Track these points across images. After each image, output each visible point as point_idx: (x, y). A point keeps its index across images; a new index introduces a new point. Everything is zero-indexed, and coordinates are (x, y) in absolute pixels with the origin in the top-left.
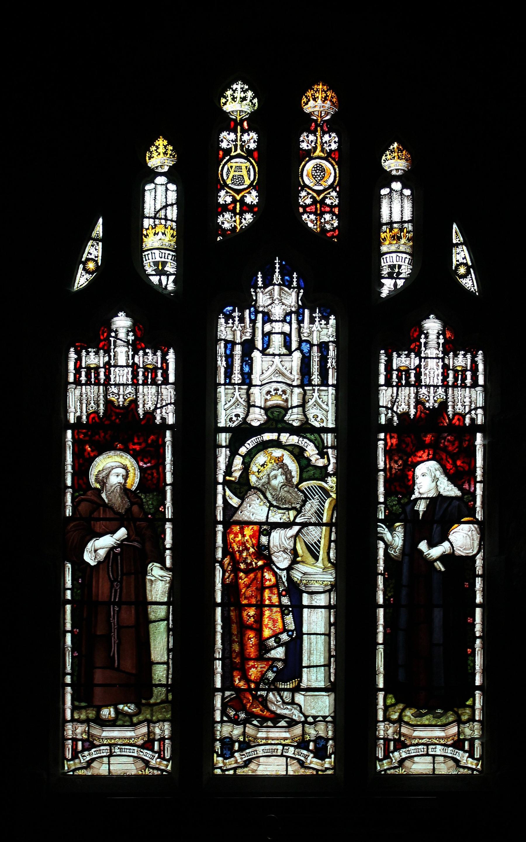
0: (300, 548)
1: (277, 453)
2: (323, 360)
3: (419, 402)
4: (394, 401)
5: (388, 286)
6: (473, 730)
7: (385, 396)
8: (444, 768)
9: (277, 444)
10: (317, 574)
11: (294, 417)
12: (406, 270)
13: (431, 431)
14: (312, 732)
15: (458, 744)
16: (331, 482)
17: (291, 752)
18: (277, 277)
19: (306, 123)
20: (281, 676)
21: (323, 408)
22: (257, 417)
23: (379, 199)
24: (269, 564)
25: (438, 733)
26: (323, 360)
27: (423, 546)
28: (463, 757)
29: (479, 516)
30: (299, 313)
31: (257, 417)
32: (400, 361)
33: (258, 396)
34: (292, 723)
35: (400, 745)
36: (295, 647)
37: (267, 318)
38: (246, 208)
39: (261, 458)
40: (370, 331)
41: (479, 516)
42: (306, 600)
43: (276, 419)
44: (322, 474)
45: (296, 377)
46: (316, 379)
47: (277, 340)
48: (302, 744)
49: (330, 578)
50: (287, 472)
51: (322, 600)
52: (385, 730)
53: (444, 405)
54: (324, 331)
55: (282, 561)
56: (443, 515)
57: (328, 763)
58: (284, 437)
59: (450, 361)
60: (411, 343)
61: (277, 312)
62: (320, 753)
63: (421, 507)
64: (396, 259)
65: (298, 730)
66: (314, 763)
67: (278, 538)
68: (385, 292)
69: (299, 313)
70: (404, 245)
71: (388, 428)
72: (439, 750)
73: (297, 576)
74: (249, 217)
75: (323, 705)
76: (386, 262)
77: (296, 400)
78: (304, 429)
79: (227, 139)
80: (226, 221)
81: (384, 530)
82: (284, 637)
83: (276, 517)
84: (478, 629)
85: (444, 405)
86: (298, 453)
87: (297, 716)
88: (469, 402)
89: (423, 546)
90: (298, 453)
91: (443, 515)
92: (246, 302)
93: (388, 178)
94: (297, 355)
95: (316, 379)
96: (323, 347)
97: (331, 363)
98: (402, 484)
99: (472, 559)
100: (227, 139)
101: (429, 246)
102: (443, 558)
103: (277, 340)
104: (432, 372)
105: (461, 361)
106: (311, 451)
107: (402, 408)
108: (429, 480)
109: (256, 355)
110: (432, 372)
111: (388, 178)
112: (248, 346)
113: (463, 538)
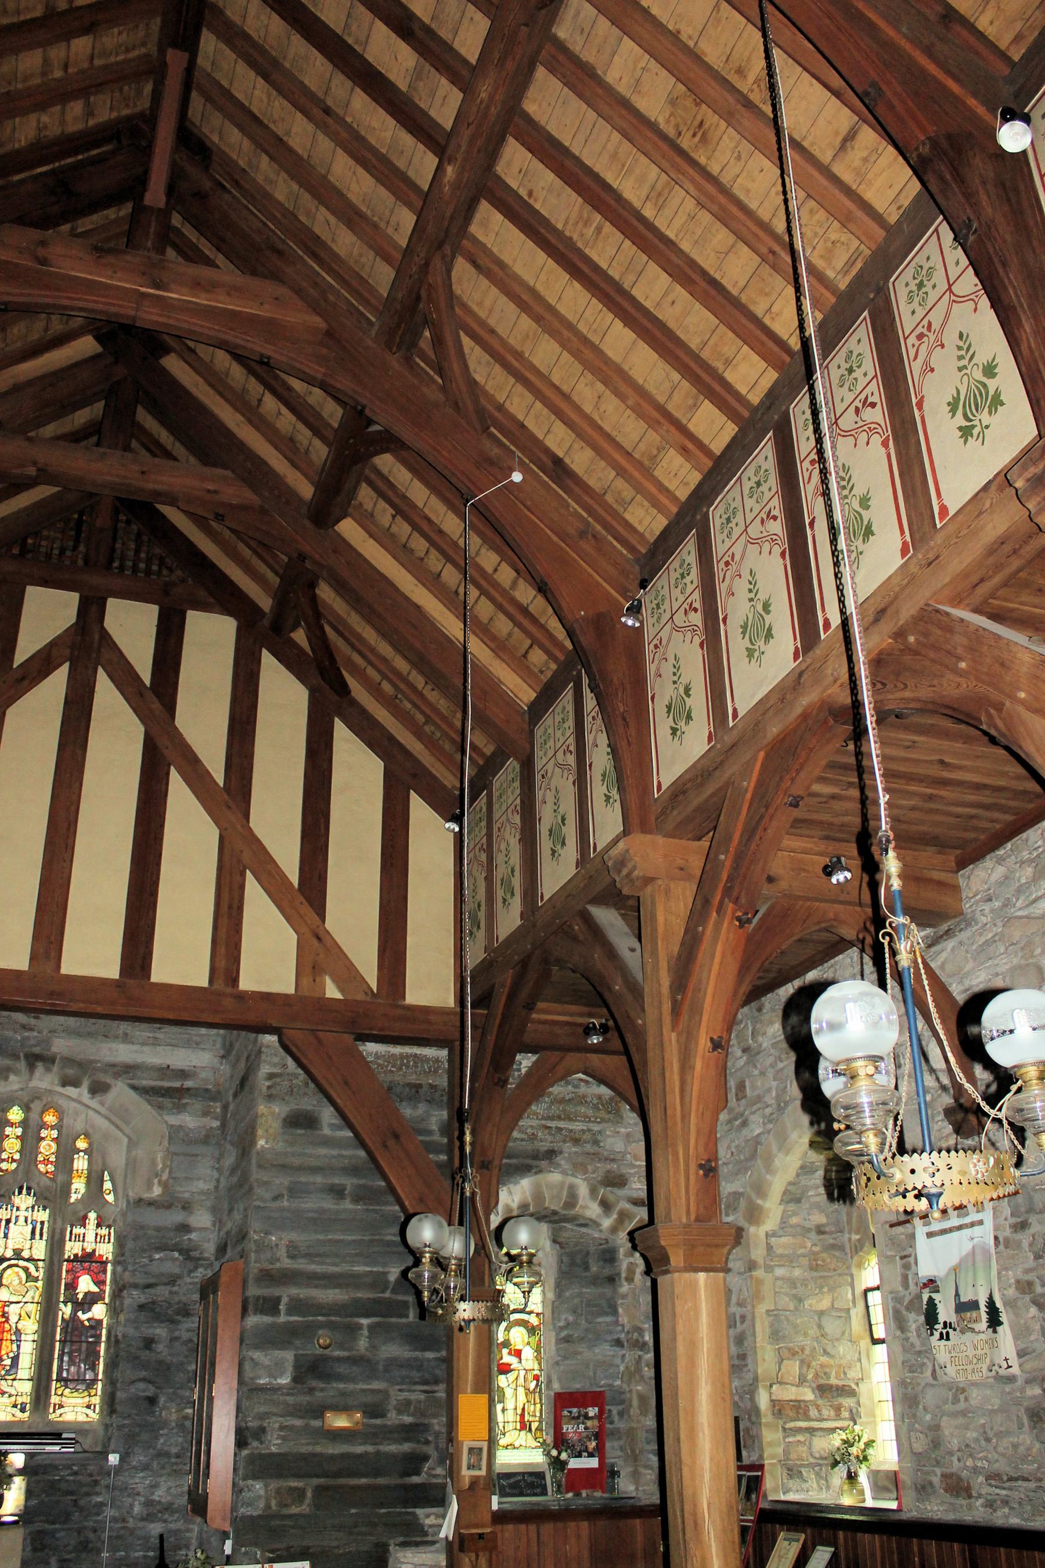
0: (23, 1314)
1: (16, 1269)
2: (42, 1229)
3: (83, 1249)
4: (72, 1248)
5: (73, 1198)
6: (96, 1400)
7: (68, 1245)
8: (82, 1418)
9: (17, 1266)
10: (30, 1327)
11: (26, 1254)
12: (83, 1190)
13: (88, 1260)
14: (20, 1400)
15: (88, 1407)
16: (40, 1284)
17: (9, 1409)
18: (24, 1191)
19: (44, 1126)
20: (8, 1372)
21: (40, 1249)
22: (9, 1254)
23: (73, 1160)
24: (7, 1320)
25: (80, 1401)
26: (42, 1229)
27: (80, 1314)
28: (89, 1412)
29: (107, 1300)
30: (33, 1207)
31: (9, 1254)
32: (77, 1230)
33: (11, 1244)
34: (10, 1396)
35: (61, 1406)
36: (15, 1360)
37: (18, 1209)
38: (13, 1160)
39: (9, 1271)
40: (64, 1216)
41: (107, 1300)
42: (23, 1337)
43: (18, 1254)
44: (36, 1279)
45: (29, 1236)
46: (37, 1236)
47: (22, 1220)
48: (15, 1406)
49: (36, 1327)
50: (20, 1279)
51: (31, 1337)
52: (55, 1399)
53: (94, 1251)
54: (43, 1215)
55: (13, 1319)
56: (91, 1300)
57: (27, 1414)
58: (21, 1263)
59: (99, 1231)
60: (83, 1221)
61: (23, 1207)
62: (23, 1410)
63: (80, 1296)
64: (79, 1187)
65: (13, 1398)
66: (20, 1415)
67: (13, 1311)
68: (72, 1200)
69: (33, 1207)
70: (83, 1180)
71: (68, 1260)
72: (79, 1409)
73: (20, 1326)
74: (15, 1165)
75: (27, 1387)
76: (74, 1187)
77: (28, 1246)
78: (30, 1260)
79: (8, 1130)
80: (4, 1166)
81: (62, 1305)
82: (11, 1355)
83: (14, 1299)
84: (102, 1353)
85: (94, 1251)
86: (26, 1270)
87: (14, 1392)
88: (106, 1250)
89: (80, 1314)
90: (26, 1270)
91: (91, 1300)
92: (9, 1202)
93: (79, 1151)
94: (30, 1227)
95: (37, 1236)
96: (42, 1223)
97: (45, 1230)
98: (72, 1286)
99: (101, 1321)
100: (8, 1130)
101: (94, 1181)
102: (89, 1320)
103: (22, 1220)
104: (90, 1237)
105: (104, 1231)
106: (32, 1269)
107: (75, 1251)
108: (85, 1284)
109: (11, 1225)
110: (90, 1237)
111: (79, 1151)
112: (8, 1221)
113: (99, 1311)
